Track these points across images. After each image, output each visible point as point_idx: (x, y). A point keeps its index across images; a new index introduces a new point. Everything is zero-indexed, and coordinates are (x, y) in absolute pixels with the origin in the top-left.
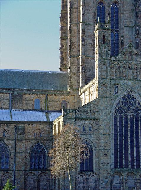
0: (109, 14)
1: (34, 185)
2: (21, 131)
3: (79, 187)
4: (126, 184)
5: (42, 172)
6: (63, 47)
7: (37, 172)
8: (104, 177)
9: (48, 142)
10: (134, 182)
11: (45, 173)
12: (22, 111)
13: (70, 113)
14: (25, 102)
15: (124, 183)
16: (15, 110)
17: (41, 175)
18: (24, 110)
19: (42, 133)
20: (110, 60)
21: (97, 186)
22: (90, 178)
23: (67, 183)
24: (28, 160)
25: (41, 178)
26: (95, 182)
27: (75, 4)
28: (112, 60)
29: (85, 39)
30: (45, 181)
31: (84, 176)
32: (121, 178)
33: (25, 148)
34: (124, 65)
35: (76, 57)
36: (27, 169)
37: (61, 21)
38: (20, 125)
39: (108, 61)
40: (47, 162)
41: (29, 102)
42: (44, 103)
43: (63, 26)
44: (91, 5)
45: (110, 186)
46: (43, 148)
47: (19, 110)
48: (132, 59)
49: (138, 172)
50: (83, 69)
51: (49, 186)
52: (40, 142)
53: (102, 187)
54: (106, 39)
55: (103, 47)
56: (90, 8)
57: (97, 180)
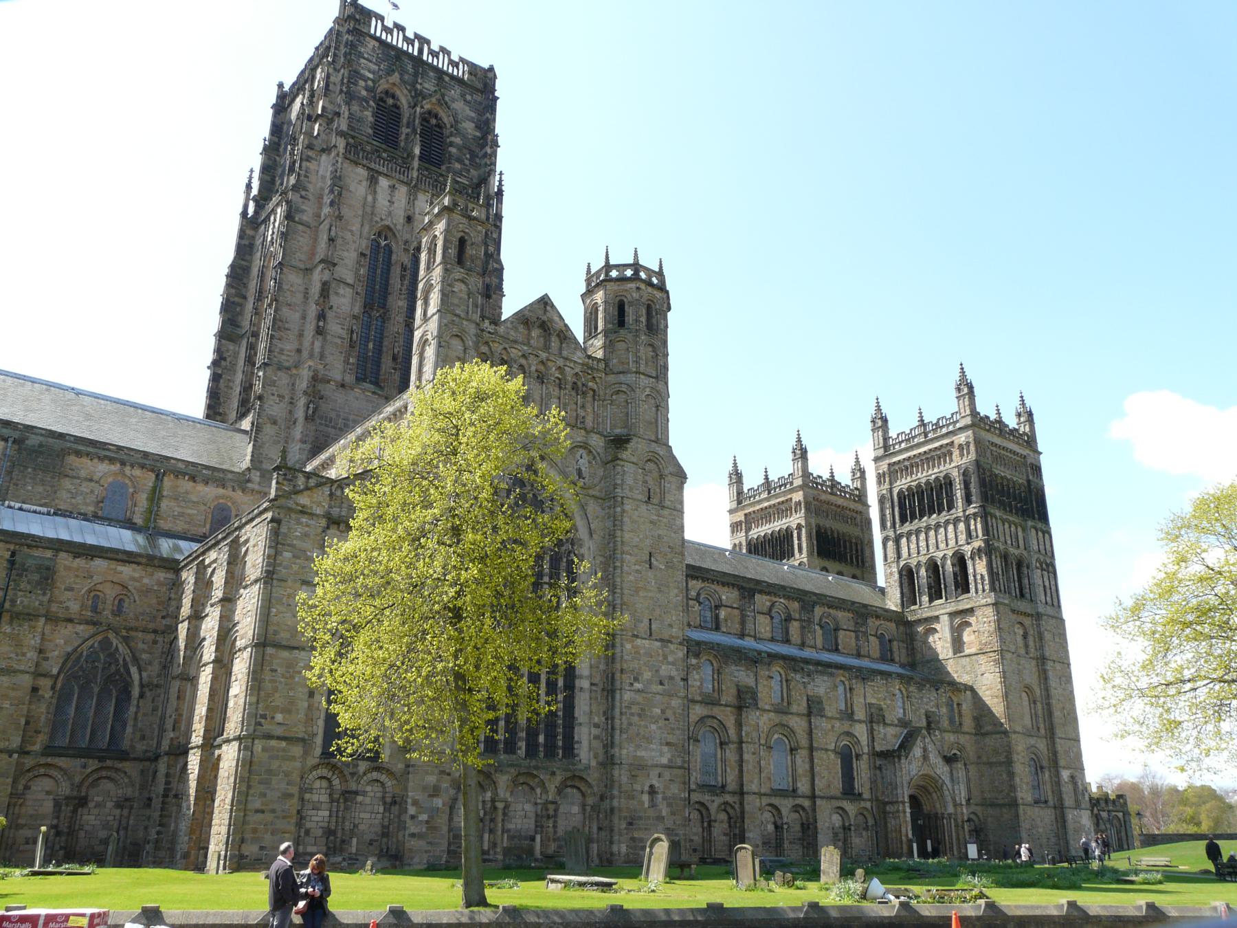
0: (404, 268)
1: (55, 822)
2: (36, 577)
3: (307, 832)
4: (503, 820)
5: (101, 765)
6: (223, 363)
7: (79, 762)
8: (425, 788)
9: (150, 637)
10: (532, 815)
11: (117, 770)
12: (48, 514)
13: (307, 488)
14: (67, 484)
15: (500, 818)
16: (18, 505)
17: (95, 776)
18: (55, 514)
19: (127, 600)
20: (478, 324)
21: (388, 827)
22: (364, 793)
23: (257, 811)
24: (43, 708)
25: (92, 792)
26: (381, 809)
27: (303, 211)
28: (483, 330)
29: (330, 315)
30: (110, 805)
31: (336, 782)
32: (489, 794)
33: (41, 651)
34: (523, 361)
35: (288, 369)
36: (29, 748)
37: (229, 286)
38: (37, 553)
39: (472, 330)
40: (130, 723)
41: (86, 487)
42: (143, 499)
43: (233, 303)
44: (354, 228)
45: (445, 829)
46: (124, 660)
47: (34, 508)
48: (546, 348)
49: (553, 774)
50: (311, 406)
51: (126, 829)
52: (111, 635)
53: (413, 835)
54: (470, 251)
55: (457, 276)
56: (348, 236)
57: (394, 803)
